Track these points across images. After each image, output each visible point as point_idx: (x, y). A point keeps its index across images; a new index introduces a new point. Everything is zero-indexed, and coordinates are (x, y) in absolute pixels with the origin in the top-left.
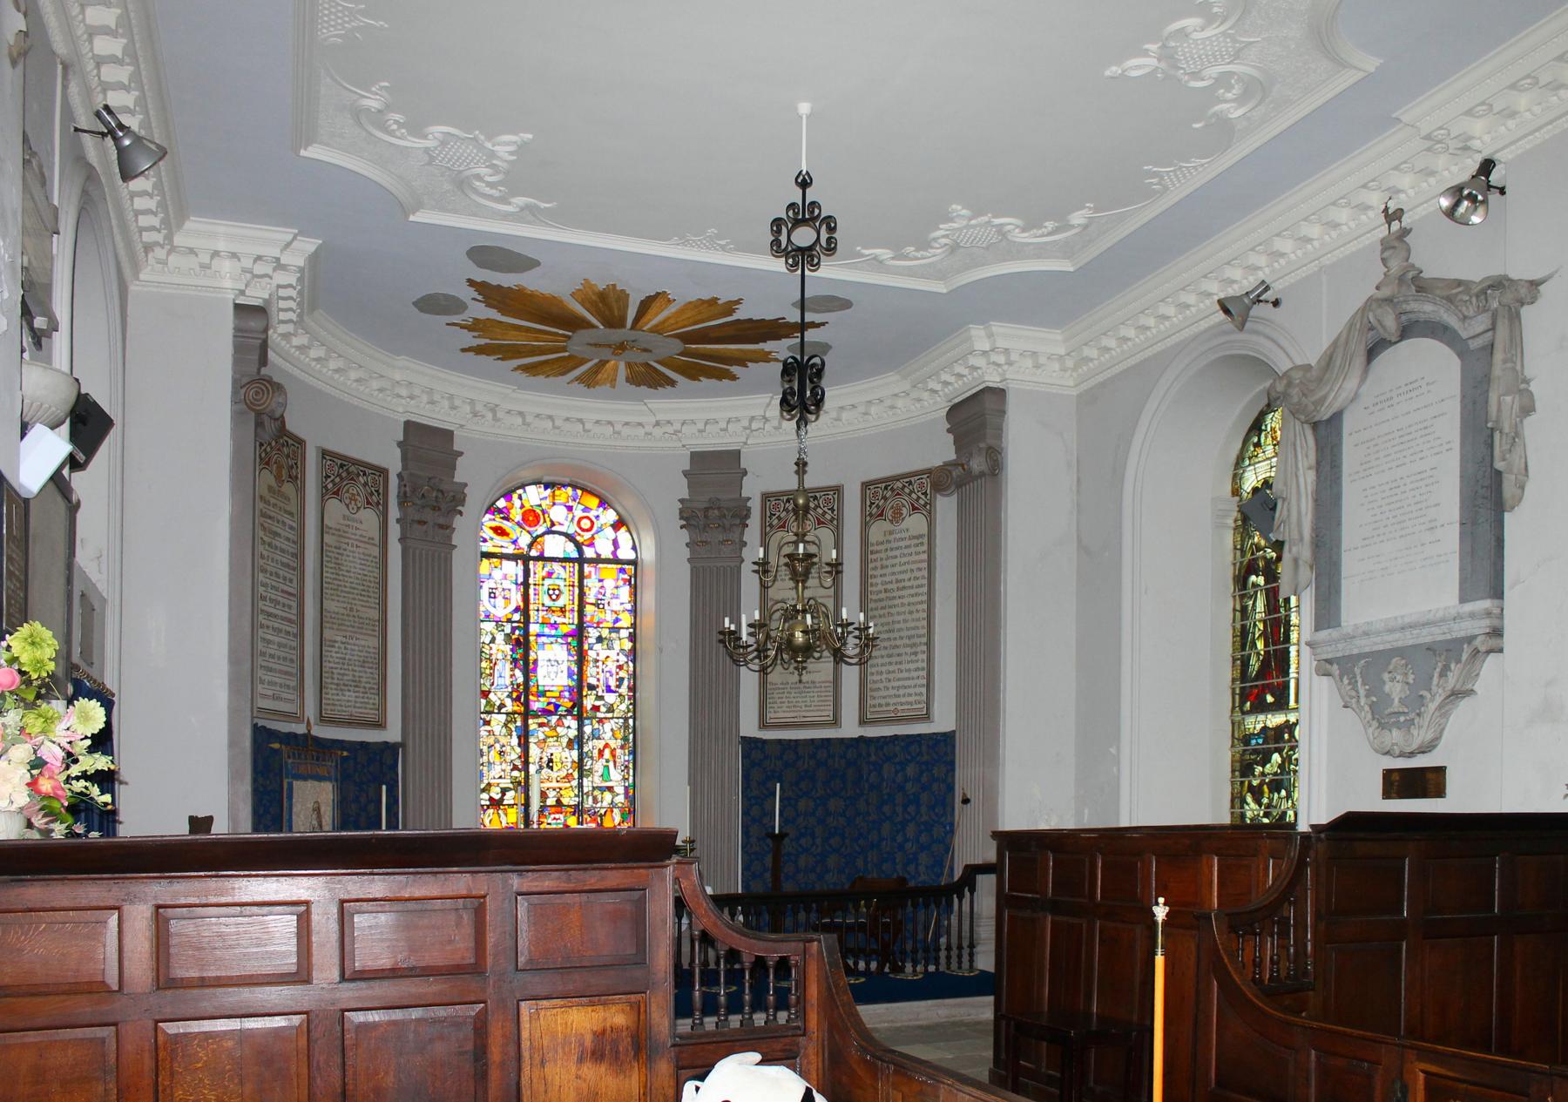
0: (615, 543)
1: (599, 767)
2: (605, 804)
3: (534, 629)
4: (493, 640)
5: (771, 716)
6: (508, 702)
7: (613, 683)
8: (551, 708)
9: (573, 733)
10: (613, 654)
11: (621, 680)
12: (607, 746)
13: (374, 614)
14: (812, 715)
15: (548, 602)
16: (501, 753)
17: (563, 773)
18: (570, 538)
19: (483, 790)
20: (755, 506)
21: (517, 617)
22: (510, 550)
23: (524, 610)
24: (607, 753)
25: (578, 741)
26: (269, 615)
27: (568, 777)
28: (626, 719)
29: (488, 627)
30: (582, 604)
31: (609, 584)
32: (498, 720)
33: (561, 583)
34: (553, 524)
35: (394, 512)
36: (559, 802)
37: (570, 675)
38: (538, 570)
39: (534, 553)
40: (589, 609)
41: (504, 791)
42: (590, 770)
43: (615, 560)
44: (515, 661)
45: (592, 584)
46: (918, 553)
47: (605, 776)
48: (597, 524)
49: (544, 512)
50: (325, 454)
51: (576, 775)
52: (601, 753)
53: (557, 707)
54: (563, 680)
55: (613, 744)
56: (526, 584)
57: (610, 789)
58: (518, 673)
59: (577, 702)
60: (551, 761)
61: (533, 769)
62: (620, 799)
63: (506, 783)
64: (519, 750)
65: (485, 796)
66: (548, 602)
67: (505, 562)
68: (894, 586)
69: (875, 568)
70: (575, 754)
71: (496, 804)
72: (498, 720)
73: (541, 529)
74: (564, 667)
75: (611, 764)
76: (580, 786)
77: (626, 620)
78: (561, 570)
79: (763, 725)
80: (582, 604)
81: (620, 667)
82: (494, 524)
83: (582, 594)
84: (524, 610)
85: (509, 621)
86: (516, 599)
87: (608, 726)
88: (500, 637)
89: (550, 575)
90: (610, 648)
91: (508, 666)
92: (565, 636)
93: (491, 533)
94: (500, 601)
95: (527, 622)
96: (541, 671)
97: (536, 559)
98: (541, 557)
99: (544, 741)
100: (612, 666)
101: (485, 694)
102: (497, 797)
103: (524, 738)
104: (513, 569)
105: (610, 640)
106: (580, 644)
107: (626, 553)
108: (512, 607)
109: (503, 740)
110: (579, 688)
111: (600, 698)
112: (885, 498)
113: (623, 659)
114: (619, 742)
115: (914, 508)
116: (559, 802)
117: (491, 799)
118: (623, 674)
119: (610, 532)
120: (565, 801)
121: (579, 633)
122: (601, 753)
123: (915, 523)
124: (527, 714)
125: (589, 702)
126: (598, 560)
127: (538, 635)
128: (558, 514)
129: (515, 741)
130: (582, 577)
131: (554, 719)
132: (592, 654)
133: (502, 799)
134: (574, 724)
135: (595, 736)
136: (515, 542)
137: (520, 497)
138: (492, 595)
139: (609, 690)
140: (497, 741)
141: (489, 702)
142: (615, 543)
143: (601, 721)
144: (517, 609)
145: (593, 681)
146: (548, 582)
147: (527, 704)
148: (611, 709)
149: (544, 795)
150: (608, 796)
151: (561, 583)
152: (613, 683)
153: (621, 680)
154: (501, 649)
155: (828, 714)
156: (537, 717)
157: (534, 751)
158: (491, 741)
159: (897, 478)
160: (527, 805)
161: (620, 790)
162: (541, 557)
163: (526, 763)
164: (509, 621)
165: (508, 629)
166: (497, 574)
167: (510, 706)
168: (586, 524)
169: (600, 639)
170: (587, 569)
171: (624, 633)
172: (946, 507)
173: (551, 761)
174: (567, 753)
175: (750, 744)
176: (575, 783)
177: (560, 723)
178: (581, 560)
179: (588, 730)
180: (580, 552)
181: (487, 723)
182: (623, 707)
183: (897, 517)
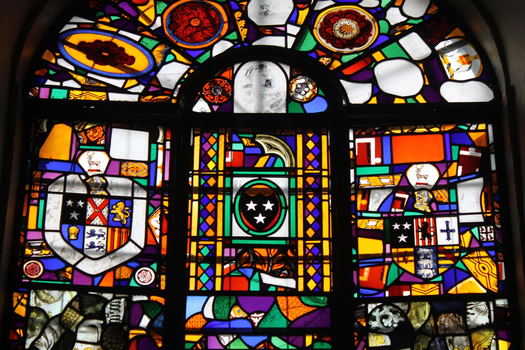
0: (434, 71)
3: (198, 307)
18: (296, 61)
23: (170, 256)
29: (56, 303)
30: (346, 233)
33: (282, 183)
34: (257, 31)
39: (201, 106)
45: (375, 185)
73: (220, 48)
77: (482, 275)
78: (281, 150)
82: (89, 38)
86: (143, 223)
89: (247, 162)
93: (81, 58)
94: (97, 235)
95: (178, 293)
97: (206, 125)
107: (464, 87)
108: (131, 250)
119: (415, 45)
126: (386, 115)
127: (209, 330)
136: (148, 79)
138: (74, 214)
142: (434, 71)
146: (239, 182)
151: (282, 183)
162: (227, 121)
164: (122, 287)
165: (116, 311)
166: (94, 161)
170: (356, 142)
171: (479, 316)
180: (336, 96)
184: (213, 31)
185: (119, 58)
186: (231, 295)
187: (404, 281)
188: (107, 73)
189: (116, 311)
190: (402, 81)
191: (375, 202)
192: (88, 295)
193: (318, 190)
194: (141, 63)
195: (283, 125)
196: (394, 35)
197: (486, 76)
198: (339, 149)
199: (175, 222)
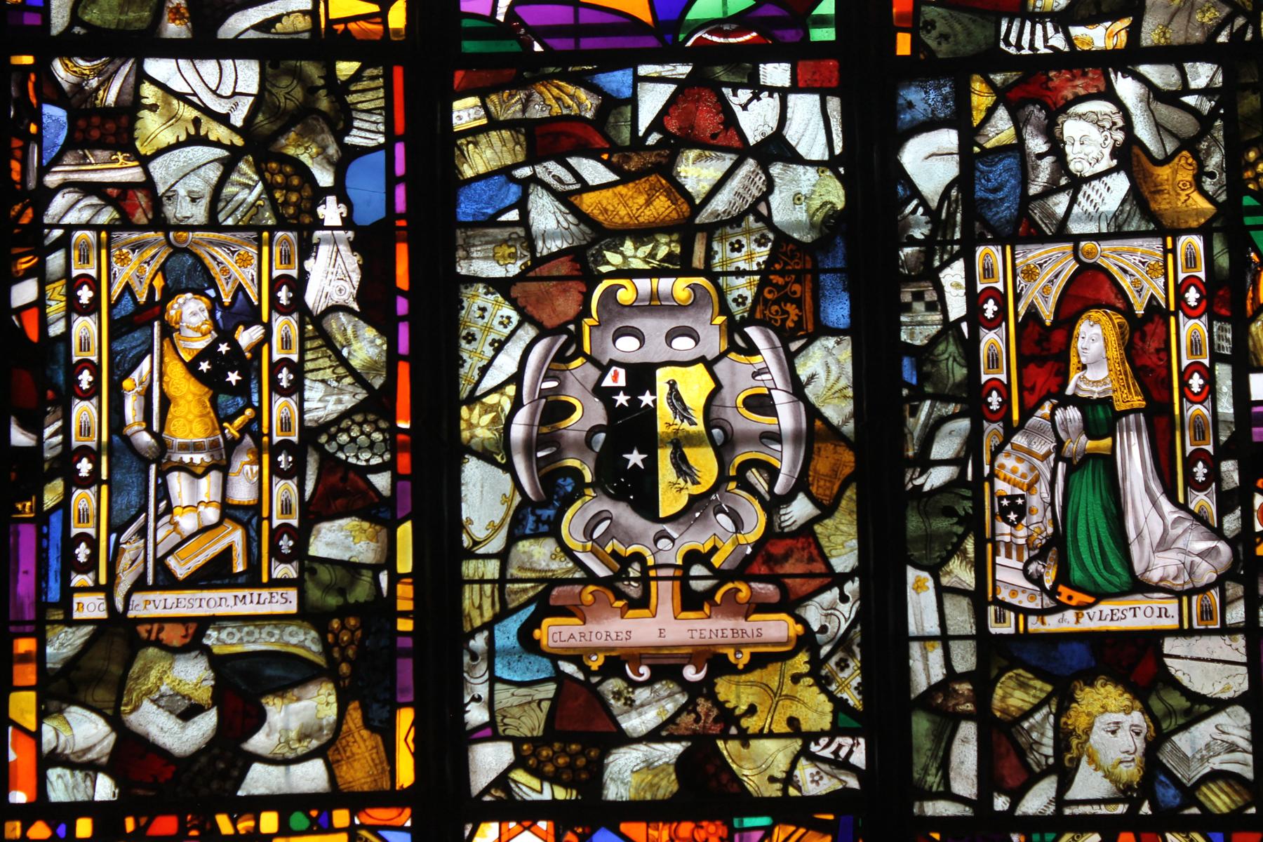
1: (1022, 467)
9: (805, 196)
12: (1089, 289)
17: (732, 534)
19: (59, 691)
24: (1094, 339)
25: (857, 262)
27: (780, 568)
41: (243, 689)
42: (970, 512)
47: (1088, 550)
52: (1045, 348)
55: (1137, 267)
57: (1134, 663)
61: (484, 497)
63: (260, 613)
64: (365, 346)
65: (85, 730)
70: (828, 366)
75: (1134, 458)
76: (882, 633)
87: (1087, 138)
99: (581, 265)
109: (237, 268)
117: (131, 754)
120: (760, 764)
129: (332, 276)
133: (228, 752)
134: (810, 124)
135: (996, 208)
140: (188, 274)
143: (1040, 90)
149: (578, 729)
150: (1112, 728)
157: (499, 354)
158: (135, 270)
173: (631, 426)
176: (832, 612)
177: (700, 120)
179: (929, 161)
181: (112, 128)
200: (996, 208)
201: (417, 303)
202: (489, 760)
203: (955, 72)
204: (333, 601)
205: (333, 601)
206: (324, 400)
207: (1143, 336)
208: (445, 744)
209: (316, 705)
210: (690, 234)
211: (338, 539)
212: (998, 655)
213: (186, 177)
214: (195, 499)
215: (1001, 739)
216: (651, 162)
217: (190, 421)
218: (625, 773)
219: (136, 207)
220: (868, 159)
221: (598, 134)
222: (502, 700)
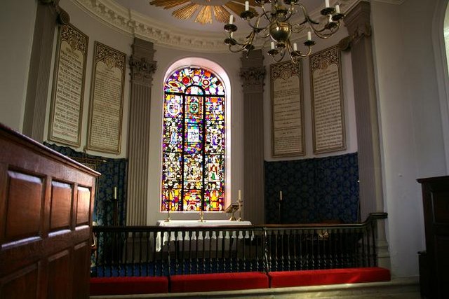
0: (217, 90)
1: (210, 174)
2: (213, 189)
3: (187, 121)
4: (171, 125)
5: (277, 152)
6: (176, 148)
7: (216, 141)
8: (192, 151)
9: (201, 161)
10: (216, 130)
11: (219, 140)
12: (214, 166)
13: (118, 108)
14: (293, 151)
15: (192, 111)
16: (173, 168)
17: (197, 176)
18: (200, 87)
19: (165, 183)
20: (268, 69)
21: (180, 116)
22: (178, 91)
25: (203, 164)
26: (63, 99)
27: (199, 178)
28: (221, 155)
29: (169, 119)
30: (205, 111)
31: (215, 104)
32: (172, 155)
34: (194, 82)
35: (128, 71)
36: (195, 188)
37: (200, 138)
38: (188, 99)
39: (187, 93)
40: (207, 113)
41: (174, 183)
42: (207, 176)
43: (217, 95)
44: (179, 133)
45: (209, 105)
46: (334, 79)
47: (213, 177)
48: (210, 83)
49: (191, 78)
50: (97, 44)
51: (202, 177)
52: (212, 168)
53: (195, 150)
54: (197, 140)
56: (184, 104)
57: (215, 183)
58: (180, 137)
59: (203, 149)
60: (192, 171)
61: (185, 174)
62: (218, 187)
63: (174, 180)
65: (166, 185)
66: (192, 111)
67: (176, 96)
68: (325, 94)
69: (316, 88)
70: (201, 169)
71: (170, 188)
72: (172, 155)
73: (189, 84)
74: (198, 135)
76: (203, 181)
79: (273, 155)
80: (205, 111)
81: (219, 135)
83: (205, 109)
84: (183, 114)
85: (177, 118)
86: (180, 109)
87: (214, 158)
88: (173, 124)
89: (192, 101)
90: (215, 128)
91: (176, 134)
92: (198, 124)
94: (174, 111)
95: (184, 118)
96: (189, 137)
97: (188, 95)
98: (189, 95)
100: (216, 135)
101: (167, 145)
102: (171, 185)
103: (183, 161)
104: (179, 99)
105: (215, 125)
106: (204, 126)
108: (179, 112)
110: (203, 142)
111: (211, 147)
112: (319, 60)
113: (220, 132)
114: (218, 164)
115: (332, 62)
116: (195, 188)
118: (219, 138)
119: (215, 86)
120: (197, 187)
121: (204, 123)
122: (212, 168)
123: (333, 68)
124: (183, 153)
125: (207, 149)
126: (210, 95)
127: (188, 123)
128: (196, 79)
129: (178, 163)
130: (205, 102)
131: (194, 155)
132: (208, 130)
133: (173, 186)
134: (201, 157)
136: (180, 89)
137: (182, 73)
138: (171, 108)
139: (214, 144)
140: (171, 163)
141: (169, 148)
142: (217, 90)
143: (211, 156)
144: (180, 113)
145: (208, 140)
146: (192, 104)
147: (183, 149)
148: (215, 151)
149: (189, 185)
150: (214, 185)
152: (216, 141)
153: (219, 140)
154: (174, 127)
155: (300, 150)
156: (187, 154)
157: (186, 168)
158: (169, 163)
159: (324, 51)
160: (183, 189)
161: (218, 183)
162: (189, 95)
163: (183, 172)
164: (177, 118)
165: (176, 121)
166: (173, 100)
167: (176, 150)
168: (206, 82)
169: (211, 125)
170: (206, 99)
171: (220, 123)
172: (347, 59)
173: (192, 171)
174: (198, 169)
175: (267, 164)
176: (201, 180)
177: (196, 157)
178: (204, 96)
179: (206, 159)
180: (204, 92)
182: (220, 151)
183: (325, 66)
184: (188, 82)
185: (176, 85)
186: (191, 119)
187: (211, 118)
188: (174, 88)
189: (176, 121)
190: (213, 91)
191: (209, 107)
192: (173, 118)
193: (201, 105)
194: (179, 87)
195: (198, 96)
196: (211, 85)
197: (224, 91)
198: (204, 100)
199: (184, 109)
200: (209, 162)
201: (182, 166)
202: (185, 187)
203: (208, 155)
204: (178, 179)
205: (178, 179)
206: (178, 169)
207: (216, 168)
208: (183, 186)
209: (177, 184)
210: (195, 162)
211: (178, 176)
212: (209, 182)
213: (171, 159)
214: (172, 174)
215: (209, 187)
216: (194, 159)
217: (171, 170)
218: (192, 188)
219: (169, 160)
220: (204, 159)
221: (191, 157)
222: (186, 184)
